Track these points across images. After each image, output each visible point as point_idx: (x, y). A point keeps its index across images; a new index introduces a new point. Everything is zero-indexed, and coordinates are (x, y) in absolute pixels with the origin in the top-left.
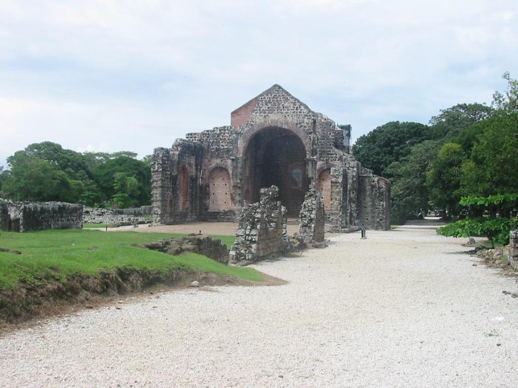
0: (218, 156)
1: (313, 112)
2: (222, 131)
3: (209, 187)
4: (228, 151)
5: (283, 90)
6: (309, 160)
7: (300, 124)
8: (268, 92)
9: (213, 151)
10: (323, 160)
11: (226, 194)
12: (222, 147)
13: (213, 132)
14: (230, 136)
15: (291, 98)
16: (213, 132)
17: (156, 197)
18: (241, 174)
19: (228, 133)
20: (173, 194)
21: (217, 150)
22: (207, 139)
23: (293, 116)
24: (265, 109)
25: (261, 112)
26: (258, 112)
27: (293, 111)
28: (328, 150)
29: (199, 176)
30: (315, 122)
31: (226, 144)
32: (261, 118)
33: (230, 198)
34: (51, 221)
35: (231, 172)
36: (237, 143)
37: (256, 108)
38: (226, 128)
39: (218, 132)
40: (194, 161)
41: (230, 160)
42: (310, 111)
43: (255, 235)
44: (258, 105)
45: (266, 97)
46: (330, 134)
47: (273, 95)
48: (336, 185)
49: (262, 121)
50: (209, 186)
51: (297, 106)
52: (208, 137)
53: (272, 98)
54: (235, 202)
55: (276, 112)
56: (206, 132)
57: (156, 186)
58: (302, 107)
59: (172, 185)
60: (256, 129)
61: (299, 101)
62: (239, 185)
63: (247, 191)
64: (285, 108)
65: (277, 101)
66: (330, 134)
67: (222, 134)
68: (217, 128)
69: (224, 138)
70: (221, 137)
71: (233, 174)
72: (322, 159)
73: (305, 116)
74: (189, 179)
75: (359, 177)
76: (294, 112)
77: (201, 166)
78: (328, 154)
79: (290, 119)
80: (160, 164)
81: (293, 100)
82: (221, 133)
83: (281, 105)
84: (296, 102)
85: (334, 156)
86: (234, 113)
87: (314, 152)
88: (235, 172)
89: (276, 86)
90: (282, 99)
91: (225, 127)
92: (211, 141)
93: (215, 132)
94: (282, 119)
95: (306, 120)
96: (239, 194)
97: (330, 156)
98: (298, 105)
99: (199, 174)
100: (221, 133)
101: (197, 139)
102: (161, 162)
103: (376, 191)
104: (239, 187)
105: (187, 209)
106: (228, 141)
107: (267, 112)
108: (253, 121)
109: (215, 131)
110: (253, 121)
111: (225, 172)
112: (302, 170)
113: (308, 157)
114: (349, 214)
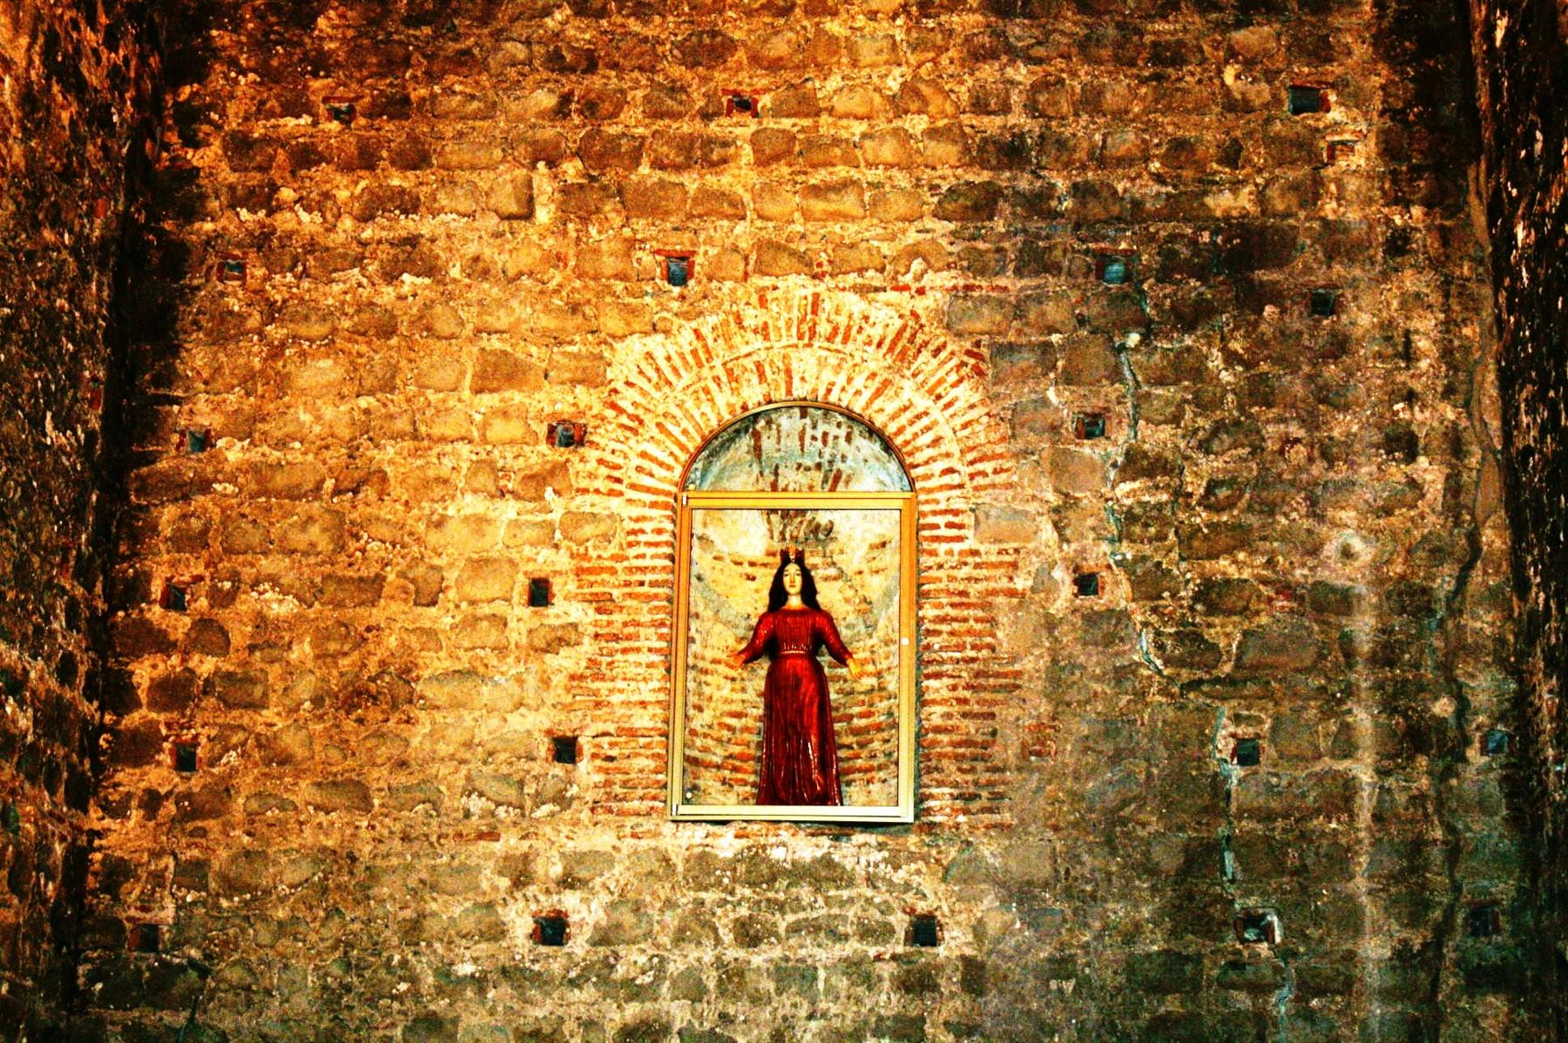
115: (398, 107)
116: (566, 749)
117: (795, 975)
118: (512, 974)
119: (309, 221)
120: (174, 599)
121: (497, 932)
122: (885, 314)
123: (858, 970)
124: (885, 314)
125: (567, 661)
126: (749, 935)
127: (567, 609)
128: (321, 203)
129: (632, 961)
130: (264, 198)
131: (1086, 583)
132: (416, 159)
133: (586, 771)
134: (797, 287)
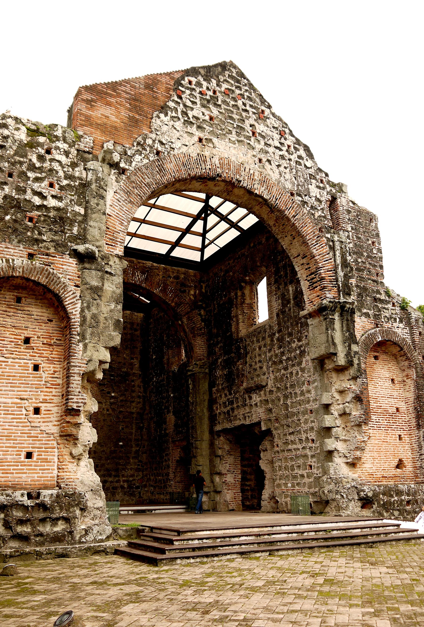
1: (327, 175)
7: (300, 195)
10: (367, 315)
11: (37, 411)
12: (37, 201)
14: (74, 165)
19: (67, 154)
23: (282, 169)
24: (200, 116)
25: (188, 123)
26: (179, 119)
27: (281, 153)
30: (333, 201)
31: (55, 191)
32: (186, 139)
33: (55, 430)
36: (103, 197)
41: (73, 262)
42: (320, 170)
44: (181, 98)
45: (205, 84)
46: (373, 243)
47: (225, 86)
51: (288, 142)
53: (225, 94)
54: (78, 450)
58: (302, 152)
66: (373, 243)
69: (47, 165)
70: (34, 159)
71: (84, 319)
72: (365, 311)
81: (272, 121)
82: (32, 145)
85: (390, 306)
88: (94, 310)
97: (380, 306)
98: (290, 141)
100: (32, 145)
106: (65, 182)
107: (207, 128)
108: (162, 143)
110: (162, 143)
131: (108, 410)
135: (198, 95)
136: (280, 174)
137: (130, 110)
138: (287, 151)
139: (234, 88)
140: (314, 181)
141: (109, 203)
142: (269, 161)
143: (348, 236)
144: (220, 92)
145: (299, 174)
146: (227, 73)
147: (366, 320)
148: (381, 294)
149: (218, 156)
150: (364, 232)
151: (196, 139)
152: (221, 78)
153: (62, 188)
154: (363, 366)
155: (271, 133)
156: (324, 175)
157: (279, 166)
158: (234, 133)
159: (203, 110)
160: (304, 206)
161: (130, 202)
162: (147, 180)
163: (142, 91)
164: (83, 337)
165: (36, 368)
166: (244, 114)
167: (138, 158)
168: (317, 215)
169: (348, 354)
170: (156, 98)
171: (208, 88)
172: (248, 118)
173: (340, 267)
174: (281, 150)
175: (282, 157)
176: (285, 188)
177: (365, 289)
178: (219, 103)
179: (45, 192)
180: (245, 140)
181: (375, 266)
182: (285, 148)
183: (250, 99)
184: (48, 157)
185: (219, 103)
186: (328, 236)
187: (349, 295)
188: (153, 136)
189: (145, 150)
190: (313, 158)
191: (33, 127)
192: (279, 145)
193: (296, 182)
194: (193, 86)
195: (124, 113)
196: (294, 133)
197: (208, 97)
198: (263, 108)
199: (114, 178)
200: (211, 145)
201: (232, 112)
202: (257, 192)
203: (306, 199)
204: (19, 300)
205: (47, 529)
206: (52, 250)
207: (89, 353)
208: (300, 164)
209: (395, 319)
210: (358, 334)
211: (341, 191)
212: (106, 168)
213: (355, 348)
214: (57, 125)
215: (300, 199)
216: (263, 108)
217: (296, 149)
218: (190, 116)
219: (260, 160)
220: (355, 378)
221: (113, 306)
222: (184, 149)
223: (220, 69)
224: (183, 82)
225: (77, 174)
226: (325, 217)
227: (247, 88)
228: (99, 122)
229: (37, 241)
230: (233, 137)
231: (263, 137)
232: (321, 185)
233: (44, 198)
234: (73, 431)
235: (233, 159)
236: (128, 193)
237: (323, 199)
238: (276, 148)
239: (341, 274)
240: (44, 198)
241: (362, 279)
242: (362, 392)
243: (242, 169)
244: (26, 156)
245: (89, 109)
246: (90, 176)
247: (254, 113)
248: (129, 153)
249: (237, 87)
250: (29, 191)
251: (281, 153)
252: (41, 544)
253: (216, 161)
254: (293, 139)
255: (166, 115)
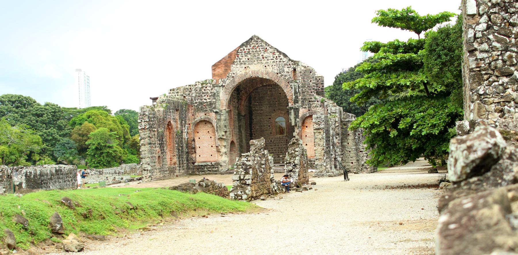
0: (202, 110)
2: (204, 85)
3: (194, 141)
4: (211, 104)
5: (262, 41)
6: (291, 108)
7: (280, 73)
8: (247, 43)
9: (196, 105)
10: (305, 108)
12: (205, 101)
13: (196, 85)
14: (212, 89)
15: (270, 48)
16: (196, 85)
17: (145, 154)
18: (225, 126)
19: (210, 87)
20: (161, 150)
21: (201, 103)
22: (189, 94)
23: (274, 66)
24: (245, 60)
27: (273, 61)
28: (309, 98)
29: (184, 131)
31: (209, 97)
32: (241, 69)
33: (216, 150)
34: (50, 183)
35: (215, 125)
37: (236, 60)
38: (208, 82)
39: (200, 86)
40: (178, 116)
41: (214, 113)
42: (290, 60)
43: (249, 179)
44: (238, 57)
45: (245, 48)
46: (311, 81)
47: (252, 46)
48: (319, 131)
49: (243, 73)
50: (194, 140)
51: (276, 55)
52: (190, 92)
53: (253, 48)
54: (222, 153)
55: (256, 62)
56: (187, 87)
57: (145, 143)
58: (282, 57)
59: (159, 141)
60: (237, 81)
61: (278, 51)
62: (224, 137)
63: (232, 143)
64: (265, 59)
65: (256, 51)
66: (311, 81)
67: (204, 88)
68: (199, 82)
69: (206, 91)
70: (203, 91)
71: (217, 127)
72: (304, 106)
73: (285, 65)
74: (175, 135)
75: (341, 121)
76: (274, 62)
77: (185, 122)
78: (310, 101)
79: (270, 69)
80: (147, 121)
82: (202, 88)
83: (261, 55)
84: (276, 51)
85: (316, 102)
86: (215, 66)
87: (296, 101)
88: (219, 124)
89: (255, 36)
90: (261, 50)
91: (206, 81)
92: (194, 95)
93: (196, 86)
94: (263, 69)
95: (286, 69)
96: (225, 146)
97: (311, 103)
99: (184, 128)
100: (202, 88)
101: (179, 94)
102: (148, 120)
103: (359, 134)
104: (224, 139)
105: (175, 164)
106: (210, 94)
107: (247, 63)
109: (196, 85)
110: (234, 73)
111: (209, 125)
112: (285, 118)
113: (290, 105)
114: (333, 159)
115: (260, 102)
116: (271, 133)
117: (281, 142)
118: (270, 143)
119: (257, 108)
120: (253, 127)
121: (269, 141)
122: (284, 112)
123: (284, 142)
124: (284, 112)
125: (271, 129)
126: (279, 141)
127: (271, 127)
128: (257, 108)
129: (275, 142)
130: (255, 107)
132: (262, 105)
133: (272, 134)
134: (280, 111)
135: (243, 53)
136: (273, 68)
137: (225, 67)
138: (276, 59)
139: (255, 45)
140: (286, 66)
141: (221, 96)
142: (269, 65)
143: (300, 82)
144: (251, 49)
145: (280, 65)
146: (253, 40)
147: (304, 109)
148: (312, 99)
149: (251, 71)
150: (307, 78)
151: (244, 68)
152: (251, 43)
153: (210, 96)
154: (300, 125)
155: (269, 55)
156: (291, 62)
157: (272, 66)
158: (256, 61)
159: (246, 57)
160: (281, 77)
161: (226, 94)
162: (230, 86)
163: (227, 59)
164: (217, 131)
165: (211, 137)
166: (259, 53)
167: (227, 81)
168: (287, 78)
169: (295, 122)
170: (232, 60)
171: (247, 49)
172: (260, 53)
173: (293, 95)
174: (273, 59)
175: (274, 62)
176: (274, 73)
177: (305, 99)
178: (251, 53)
179: (207, 99)
180: (260, 62)
181: (311, 89)
182: (274, 58)
183: (261, 46)
184: (206, 89)
185: (251, 53)
186: (291, 84)
187: (298, 103)
188: (231, 72)
189: (229, 77)
190: (287, 57)
191: (202, 83)
192: (272, 58)
193: (279, 69)
194: (242, 51)
195: (223, 69)
196: (280, 50)
197: (247, 52)
198: (266, 47)
199: (221, 89)
200: (248, 68)
201: (255, 54)
202: (264, 78)
203: (282, 74)
204: (206, 123)
205: (214, 169)
206: (210, 112)
207: (219, 134)
208: (281, 61)
209: (318, 107)
210: (300, 115)
211: (298, 65)
212: (219, 88)
213: (298, 120)
214: (207, 80)
215: (280, 74)
216: (266, 47)
217: (279, 56)
218: (241, 62)
219: (265, 66)
220: (298, 129)
221: (224, 122)
222: (240, 73)
223: (250, 40)
224: (239, 51)
225: (213, 91)
226: (290, 78)
227: (260, 42)
228: (217, 74)
229: (206, 110)
230: (256, 62)
231: (266, 58)
232: (289, 66)
233: (206, 100)
234: (219, 150)
235: (256, 70)
236: (225, 92)
237: (290, 71)
238: (271, 59)
239: (294, 97)
240: (206, 100)
241: (304, 95)
242: (299, 133)
243: (259, 72)
244: (201, 91)
245: (214, 72)
246: (215, 91)
247: (263, 50)
248: (225, 80)
249: (256, 44)
250: (203, 99)
251: (273, 61)
252: (213, 172)
253: (250, 73)
254: (278, 53)
255: (234, 64)
